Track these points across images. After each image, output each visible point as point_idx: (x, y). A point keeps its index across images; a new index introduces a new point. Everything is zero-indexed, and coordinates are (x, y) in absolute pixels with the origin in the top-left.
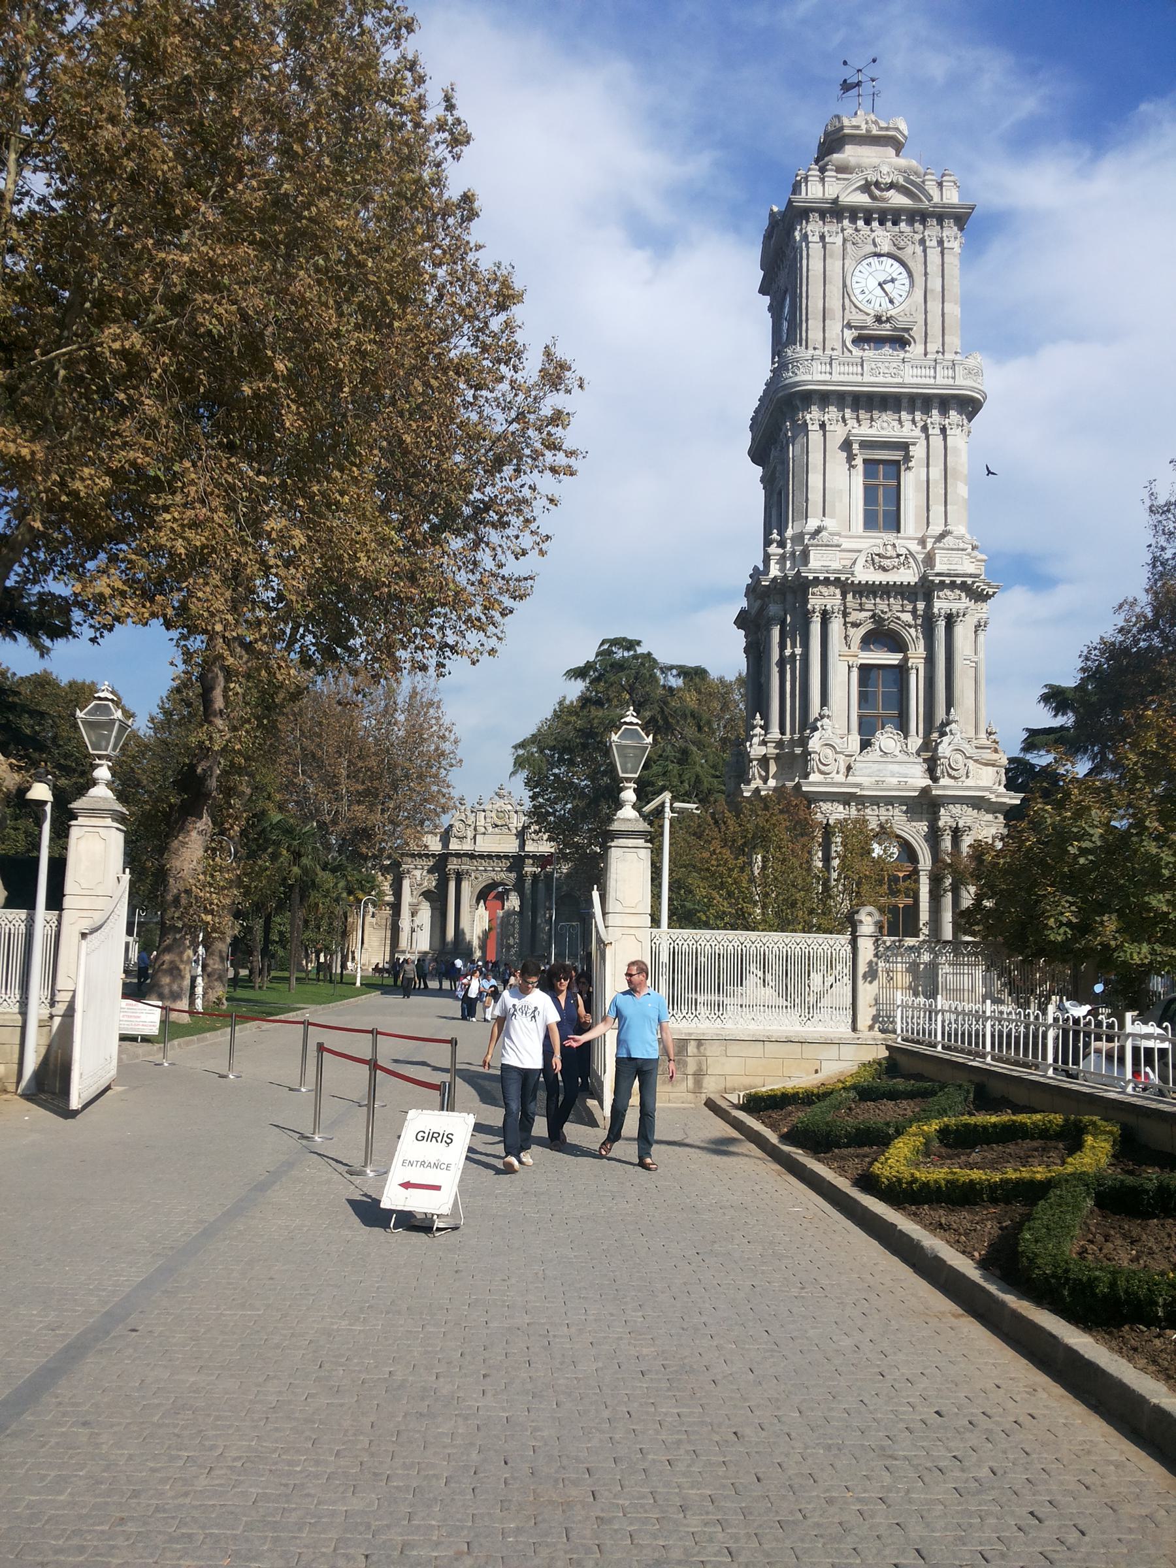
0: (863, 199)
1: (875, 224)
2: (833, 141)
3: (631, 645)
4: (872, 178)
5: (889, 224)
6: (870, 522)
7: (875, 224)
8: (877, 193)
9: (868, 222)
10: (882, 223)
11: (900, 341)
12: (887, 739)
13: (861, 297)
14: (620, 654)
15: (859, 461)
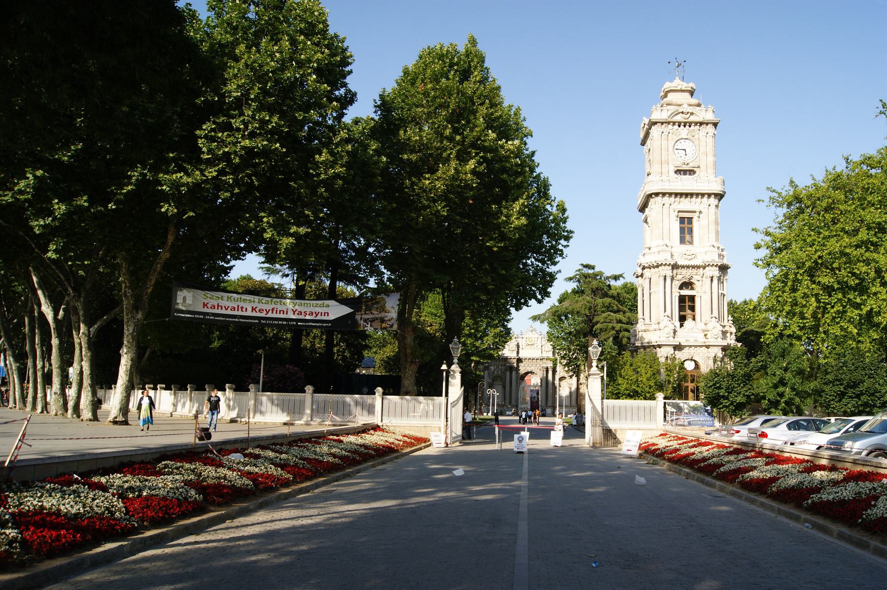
0: (679, 118)
1: (682, 127)
2: (667, 91)
3: (593, 268)
4: (680, 111)
5: (687, 127)
6: (682, 241)
7: (682, 127)
8: (684, 115)
9: (679, 126)
10: (685, 126)
11: (692, 172)
12: (689, 323)
13: (678, 155)
14: (586, 271)
15: (679, 219)
